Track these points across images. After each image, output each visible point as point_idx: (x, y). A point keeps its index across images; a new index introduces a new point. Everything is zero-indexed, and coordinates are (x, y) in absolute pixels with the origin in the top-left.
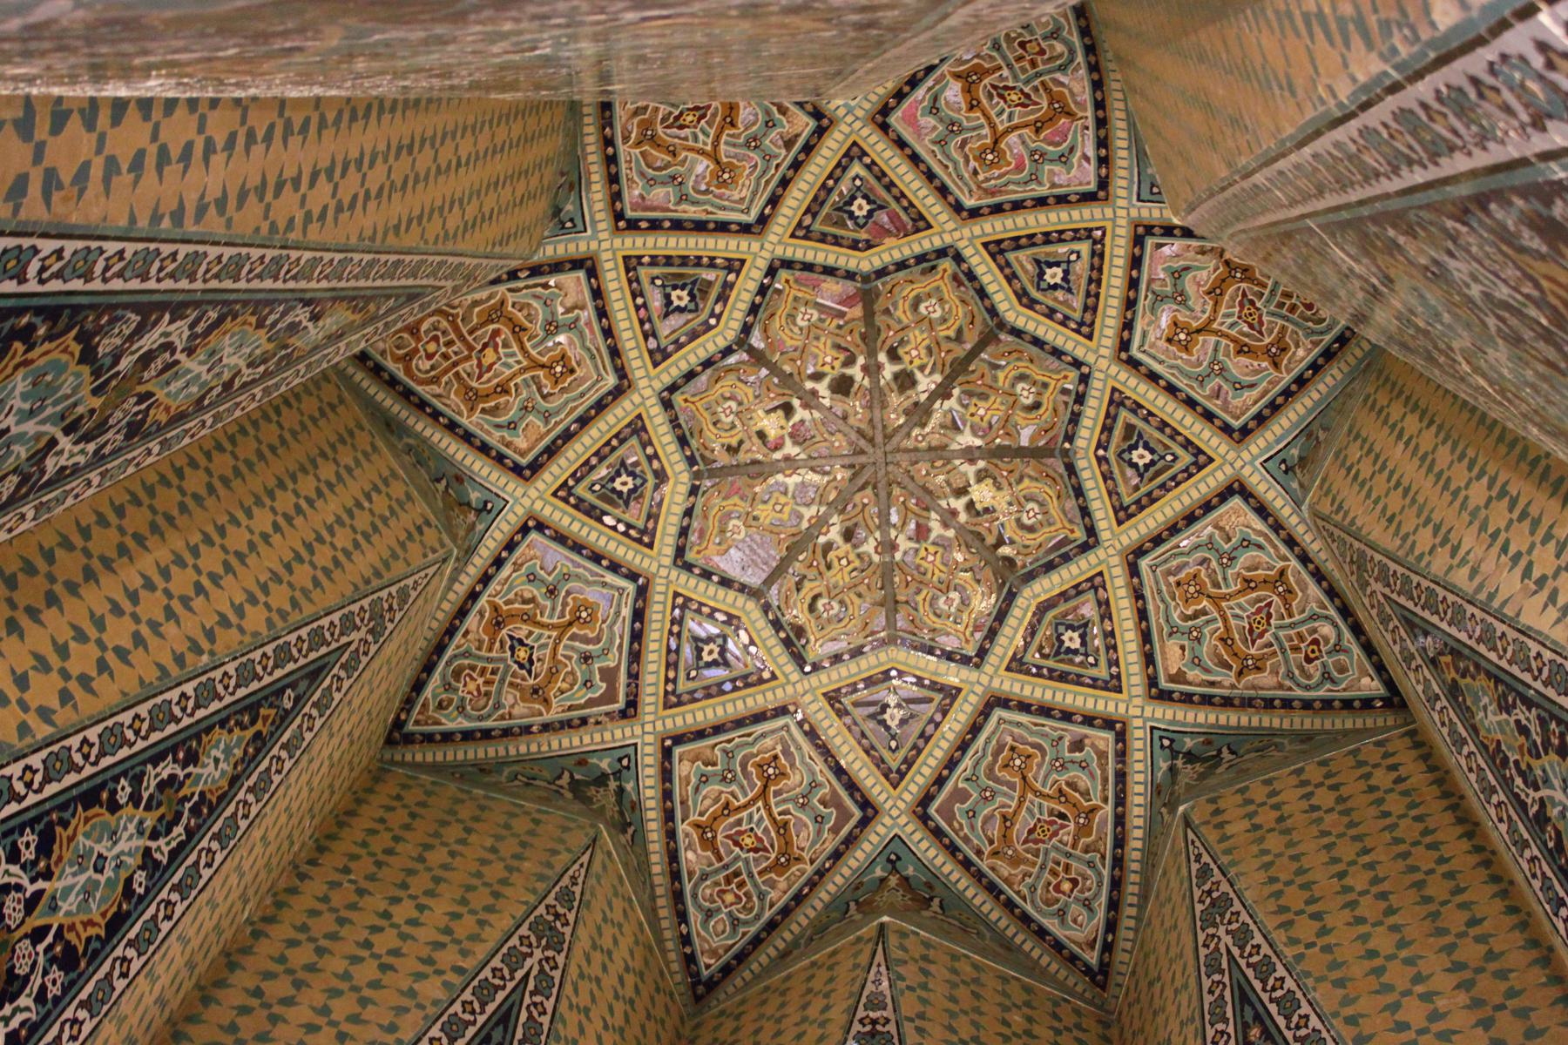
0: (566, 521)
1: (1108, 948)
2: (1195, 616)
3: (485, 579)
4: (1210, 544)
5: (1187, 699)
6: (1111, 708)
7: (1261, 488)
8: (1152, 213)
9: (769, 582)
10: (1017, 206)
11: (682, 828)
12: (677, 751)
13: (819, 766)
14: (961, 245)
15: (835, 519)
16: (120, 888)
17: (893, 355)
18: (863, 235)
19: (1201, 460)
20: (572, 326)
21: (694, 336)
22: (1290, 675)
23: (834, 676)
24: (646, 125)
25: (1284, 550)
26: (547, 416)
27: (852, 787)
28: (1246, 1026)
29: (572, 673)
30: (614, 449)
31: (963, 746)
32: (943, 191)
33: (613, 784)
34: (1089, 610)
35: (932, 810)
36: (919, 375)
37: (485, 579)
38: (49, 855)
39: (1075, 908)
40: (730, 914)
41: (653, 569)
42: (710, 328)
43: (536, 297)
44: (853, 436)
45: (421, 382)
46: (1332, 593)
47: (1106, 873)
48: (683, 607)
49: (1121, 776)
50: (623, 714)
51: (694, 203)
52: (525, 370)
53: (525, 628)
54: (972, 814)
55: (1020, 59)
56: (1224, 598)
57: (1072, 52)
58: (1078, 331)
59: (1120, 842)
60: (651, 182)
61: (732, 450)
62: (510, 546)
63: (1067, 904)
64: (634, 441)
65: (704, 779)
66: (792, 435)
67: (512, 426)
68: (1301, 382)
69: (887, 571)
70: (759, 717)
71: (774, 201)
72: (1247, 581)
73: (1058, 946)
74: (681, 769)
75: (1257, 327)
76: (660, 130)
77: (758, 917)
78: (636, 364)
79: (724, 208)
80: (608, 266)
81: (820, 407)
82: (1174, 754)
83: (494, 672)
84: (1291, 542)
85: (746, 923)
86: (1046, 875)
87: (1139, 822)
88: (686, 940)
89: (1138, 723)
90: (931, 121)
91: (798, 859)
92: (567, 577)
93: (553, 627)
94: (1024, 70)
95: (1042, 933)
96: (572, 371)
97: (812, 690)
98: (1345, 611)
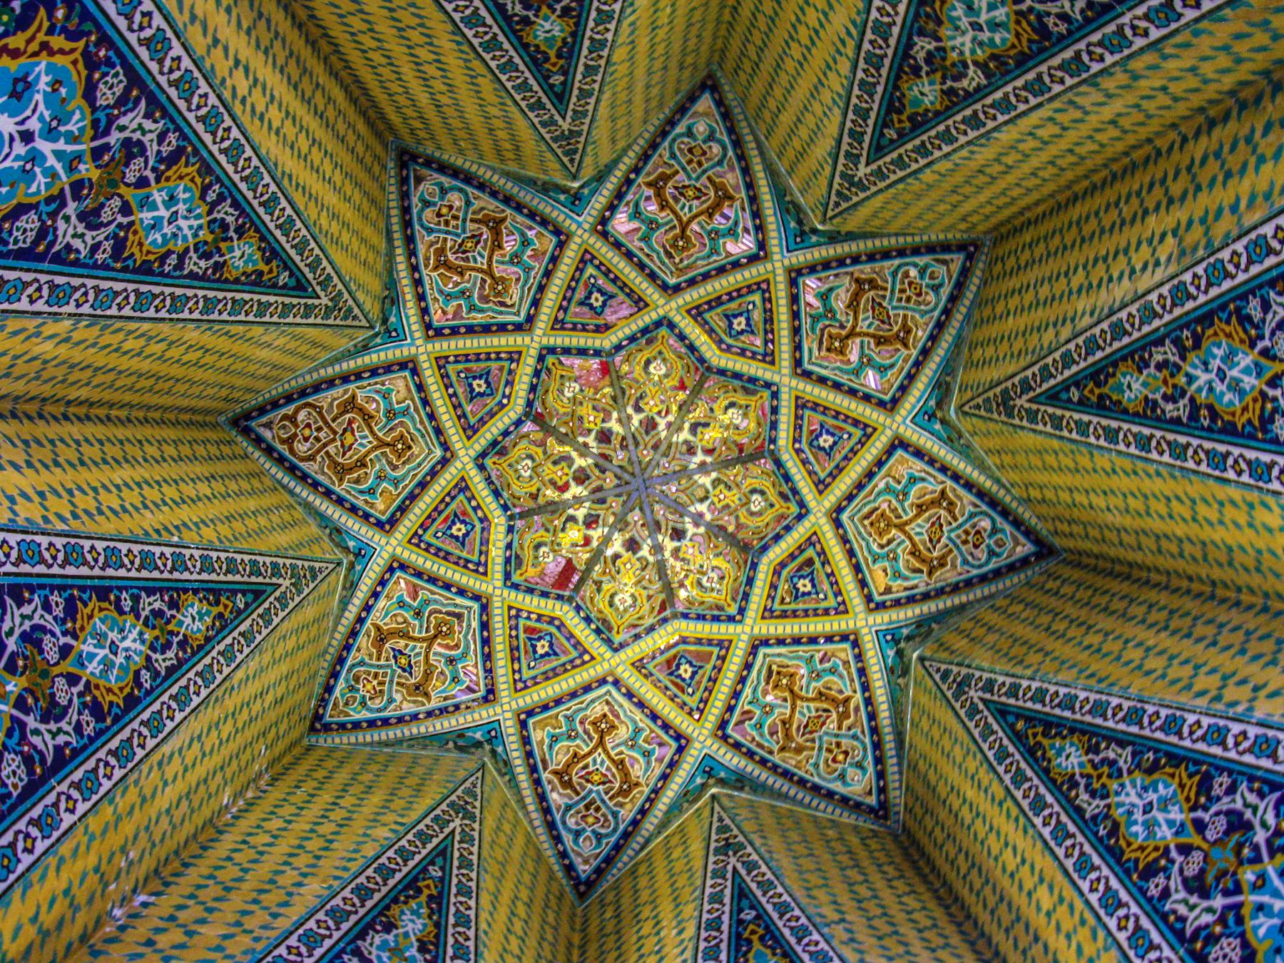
0: (421, 561)
1: (882, 790)
2: (889, 542)
3: (368, 608)
4: (888, 489)
5: (897, 603)
6: (843, 626)
7: (915, 438)
8: (801, 258)
10: (706, 276)
11: (545, 776)
12: (531, 721)
13: (638, 715)
14: (671, 315)
15: (616, 535)
16: (131, 676)
17: (638, 409)
18: (601, 322)
19: (868, 432)
22: (965, 562)
23: (637, 650)
24: (440, 252)
25: (941, 477)
26: (396, 483)
27: (666, 727)
28: (1012, 726)
29: (442, 673)
30: (448, 504)
31: (742, 680)
32: (652, 276)
33: (488, 747)
35: (729, 731)
36: (658, 419)
37: (368, 608)
38: (74, 621)
39: (851, 772)
40: (594, 831)
41: (490, 590)
42: (502, 406)
43: (377, 392)
44: (619, 471)
45: (303, 460)
46: (981, 494)
47: (867, 740)
48: (517, 616)
49: (862, 672)
50: (486, 700)
51: (481, 311)
52: (376, 448)
53: (402, 642)
54: (759, 726)
55: (690, 162)
56: (906, 523)
57: (724, 148)
58: (764, 361)
59: (872, 716)
60: (449, 297)
61: (534, 497)
62: (383, 583)
63: (844, 770)
64: (461, 497)
65: (555, 739)
66: (575, 479)
67: (371, 491)
68: (925, 352)
70: (587, 689)
71: (536, 303)
72: (919, 506)
73: (845, 800)
74: (537, 735)
75: (886, 321)
76: (451, 257)
77: (615, 830)
78: (455, 438)
79: (501, 313)
80: (426, 365)
82: (896, 641)
83: (385, 675)
84: (944, 469)
85: (607, 836)
86: (824, 753)
87: (883, 698)
88: (563, 855)
89: (865, 631)
91: (637, 784)
93: (424, 640)
94: (694, 170)
95: (830, 794)
96: (410, 448)
97: (623, 662)
98: (993, 503)
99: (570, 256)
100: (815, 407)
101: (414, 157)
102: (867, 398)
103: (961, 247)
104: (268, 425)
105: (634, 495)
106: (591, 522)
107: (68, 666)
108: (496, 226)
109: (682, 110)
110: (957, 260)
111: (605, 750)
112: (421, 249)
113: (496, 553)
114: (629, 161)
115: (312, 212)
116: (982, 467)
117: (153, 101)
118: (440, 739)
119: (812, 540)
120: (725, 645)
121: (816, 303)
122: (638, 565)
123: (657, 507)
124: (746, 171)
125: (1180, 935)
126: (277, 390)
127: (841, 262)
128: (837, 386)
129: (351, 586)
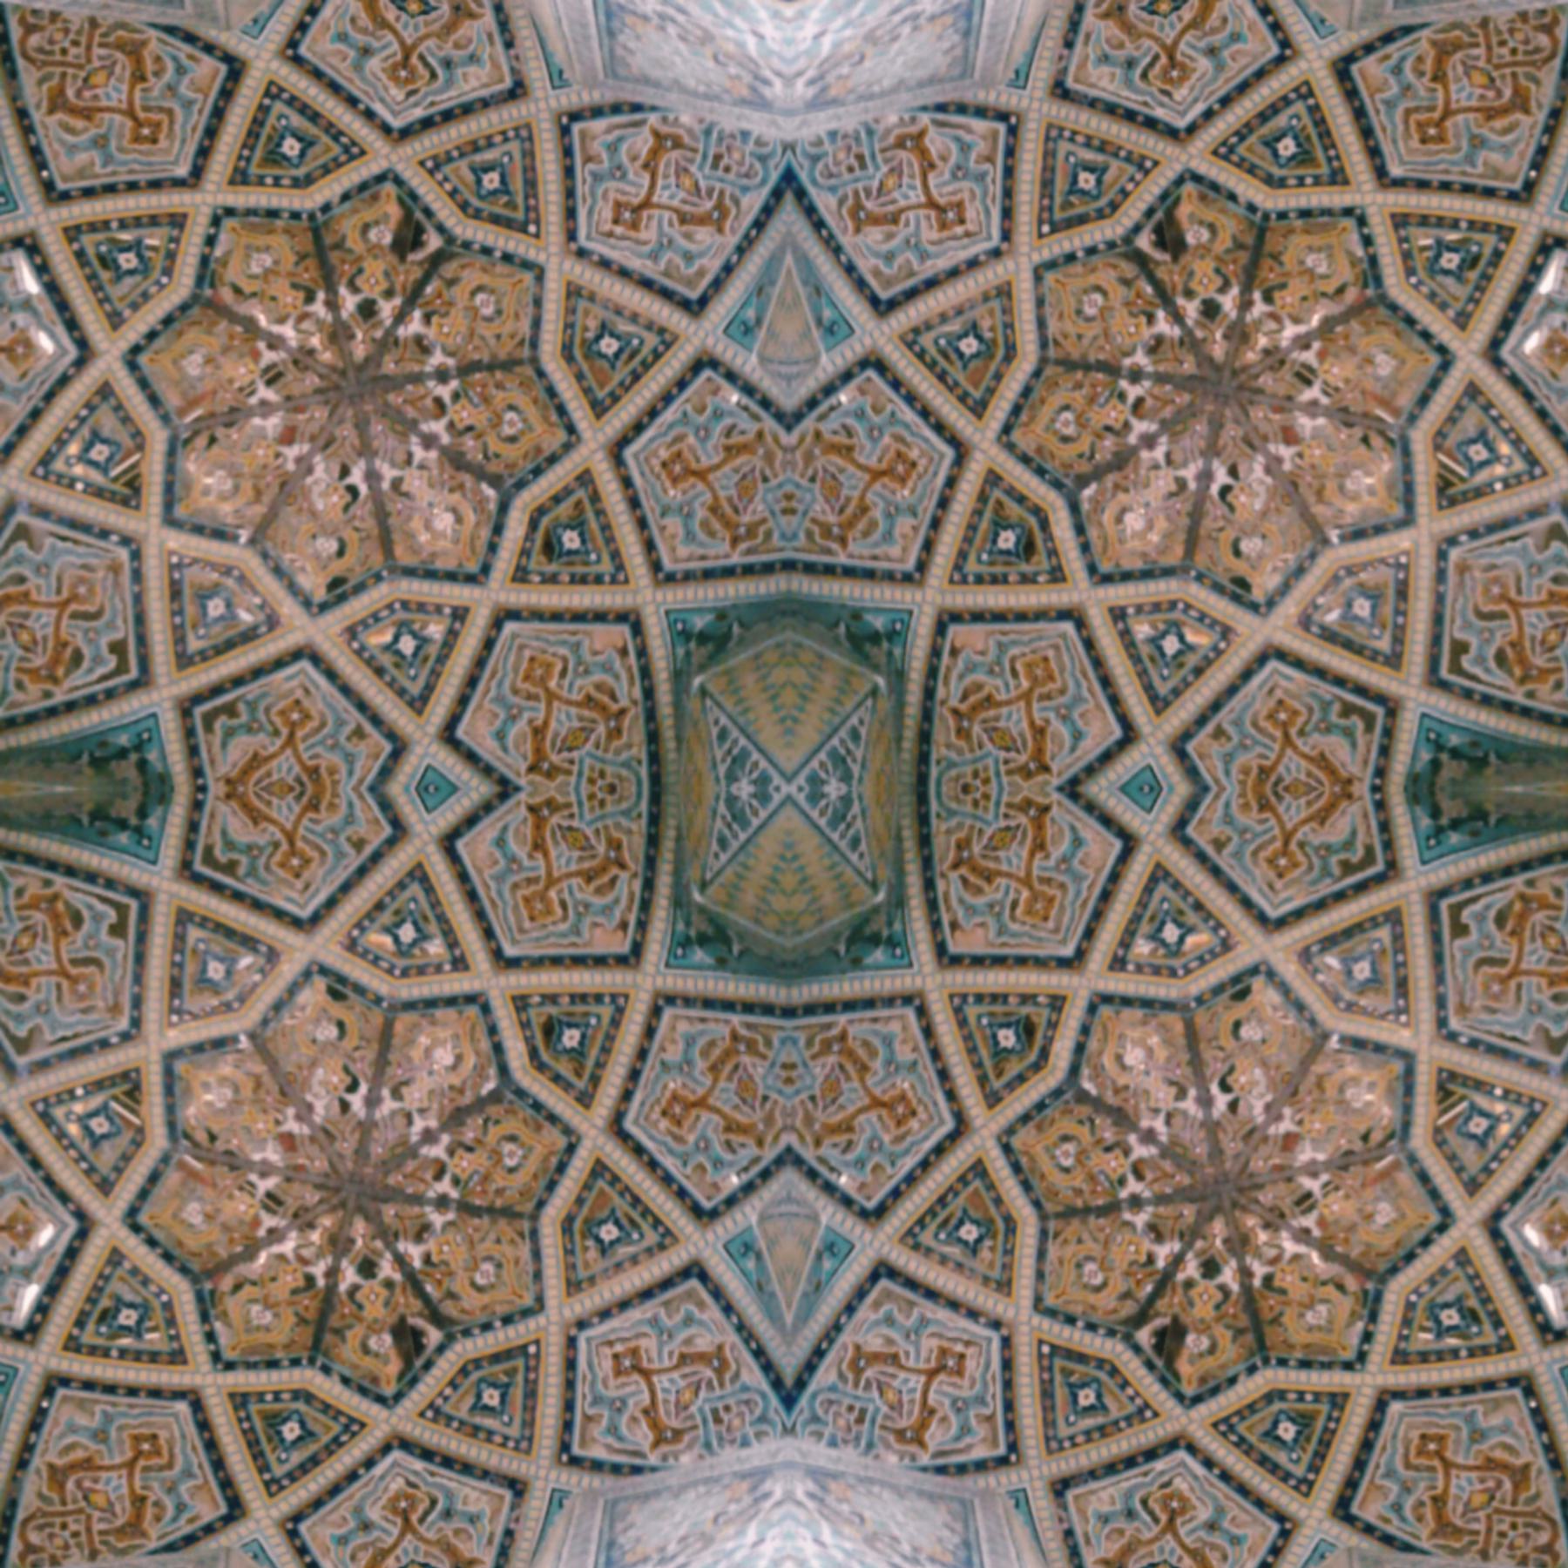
2: (563, 905)
21: (171, 1322)
29: (457, 1532)
51: (35, 1265)
52: (131, 1476)
74: (598, 1453)
81: (288, 1228)
92: (358, 1510)
105: (366, 1202)
111: (660, 1372)
119: (521, 1002)
120: (599, 1169)
122: (450, 1236)
123: (391, 1181)
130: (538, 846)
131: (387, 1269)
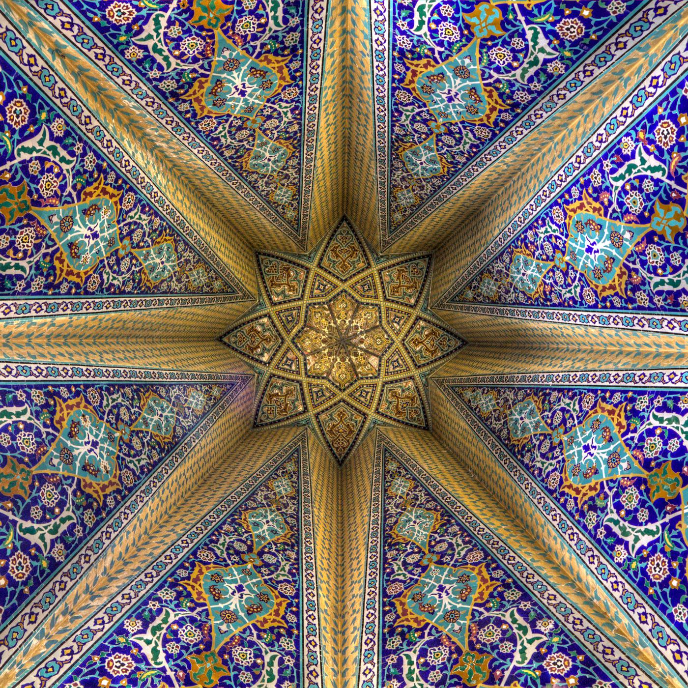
3: (391, 418)
4: (333, 267)
5: (367, 259)
9: (377, 356)
10: (277, 331)
11: (434, 358)
20: (331, 415)
24: (282, 411)
26: (352, 415)
31: (397, 302)
32: (280, 347)
34: (358, 286)
37: (391, 418)
49: (389, 267)
62: (383, 415)
65: (422, 357)
67: (356, 422)
68: (290, 262)
69: (366, 332)
70: (406, 349)
71: (293, 381)
73: (428, 268)
74: (422, 362)
84: (325, 251)
88: (456, 350)
90: (266, 354)
95: (427, 272)
99: (277, 372)
100: (312, 292)
101: (255, 423)
102: (307, 277)
103: (257, 256)
104: (340, 455)
106: (356, 355)
107: (405, 497)
108: (271, 396)
109: (229, 346)
110: (261, 257)
112: (281, 417)
113: (370, 381)
114: (246, 360)
115: (276, 450)
116: (323, 240)
117: (253, 494)
118: (426, 390)
121: (280, 297)
124: (244, 324)
125: (435, 191)
126: (329, 454)
127: (267, 291)
128: (305, 286)
129: (385, 424)
130: (337, 256)
131: (360, 352)
